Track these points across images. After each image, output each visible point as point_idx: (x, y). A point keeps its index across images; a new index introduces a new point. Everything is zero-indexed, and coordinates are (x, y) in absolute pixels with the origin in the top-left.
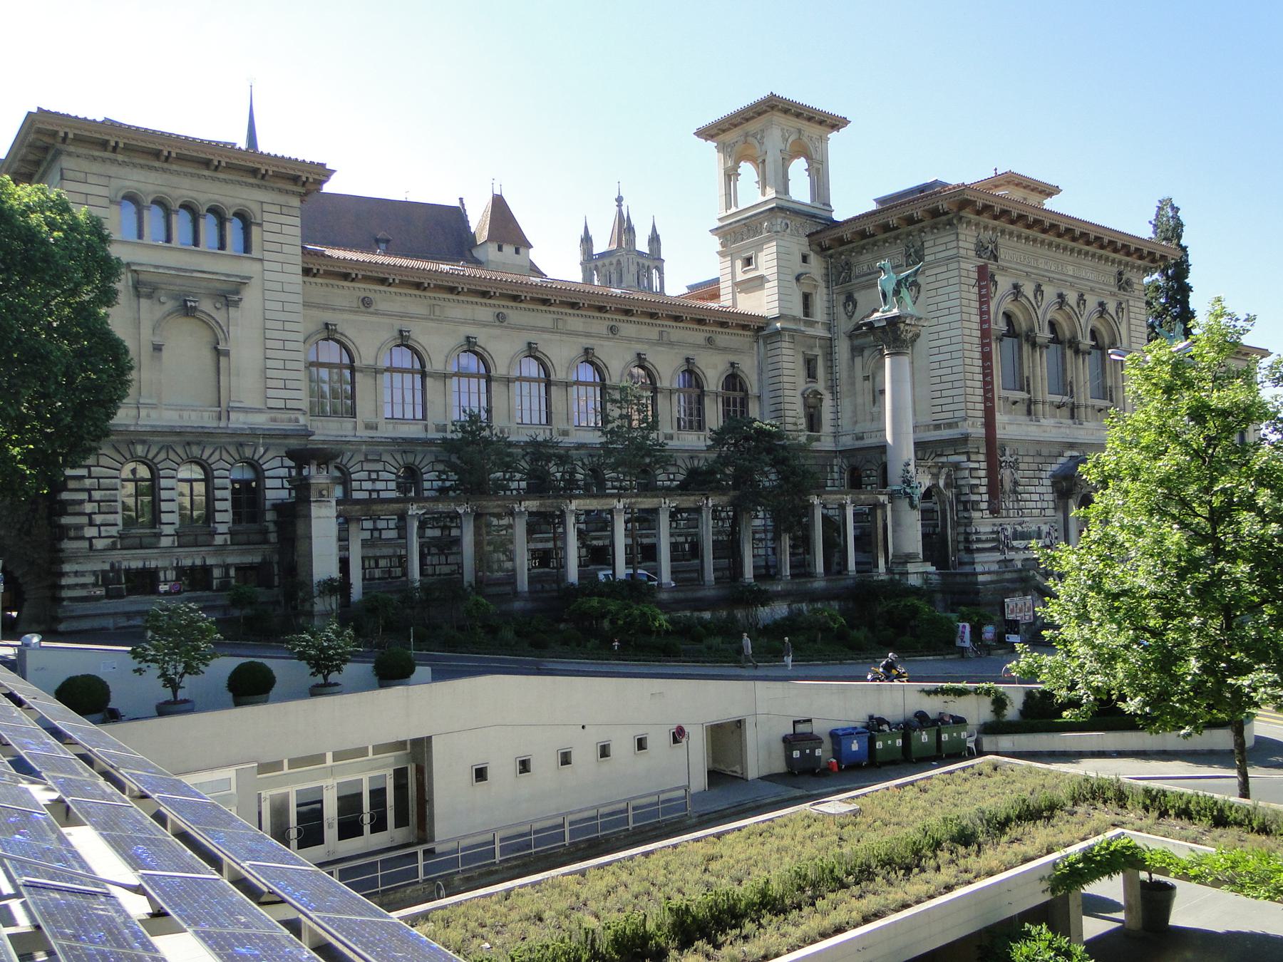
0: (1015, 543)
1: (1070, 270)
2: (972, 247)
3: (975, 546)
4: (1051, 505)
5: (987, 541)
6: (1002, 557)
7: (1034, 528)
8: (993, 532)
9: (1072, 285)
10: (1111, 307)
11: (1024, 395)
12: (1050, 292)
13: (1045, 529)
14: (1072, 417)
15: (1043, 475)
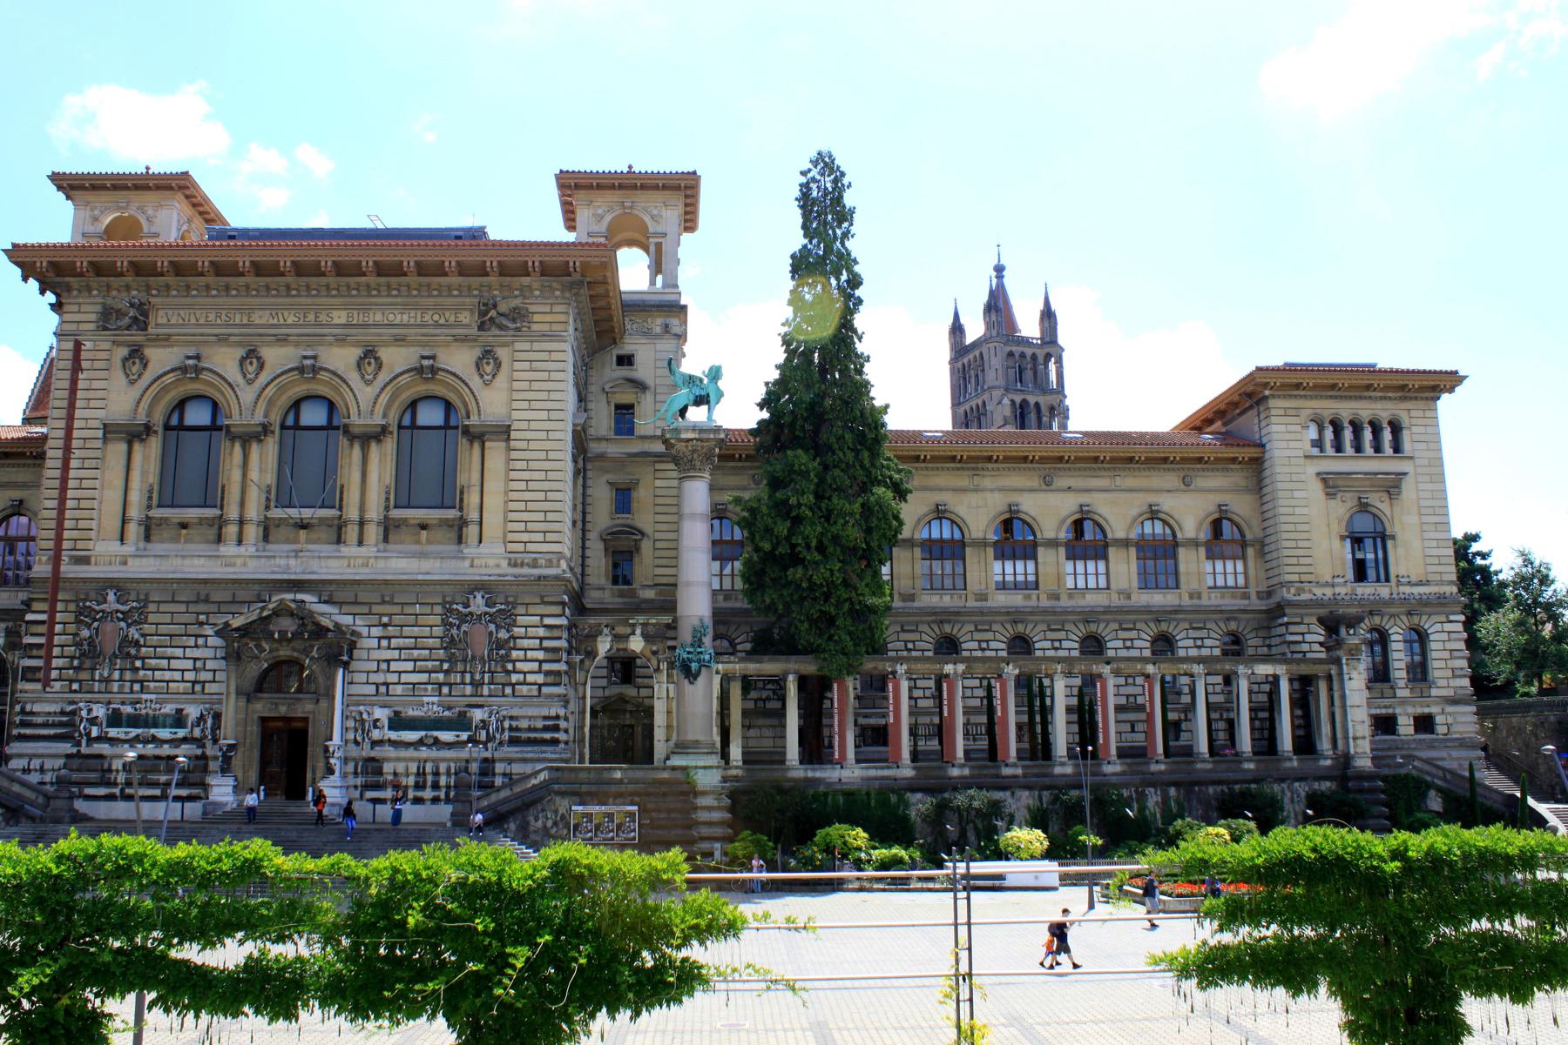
0: (113, 732)
1: (340, 317)
2: (93, 317)
3: (15, 732)
4: (220, 676)
5: (45, 725)
6: (74, 750)
7: (169, 709)
8: (63, 713)
9: (341, 341)
10: (459, 360)
11: (216, 512)
12: (277, 357)
13: (193, 712)
14: (339, 541)
15: (208, 630)
